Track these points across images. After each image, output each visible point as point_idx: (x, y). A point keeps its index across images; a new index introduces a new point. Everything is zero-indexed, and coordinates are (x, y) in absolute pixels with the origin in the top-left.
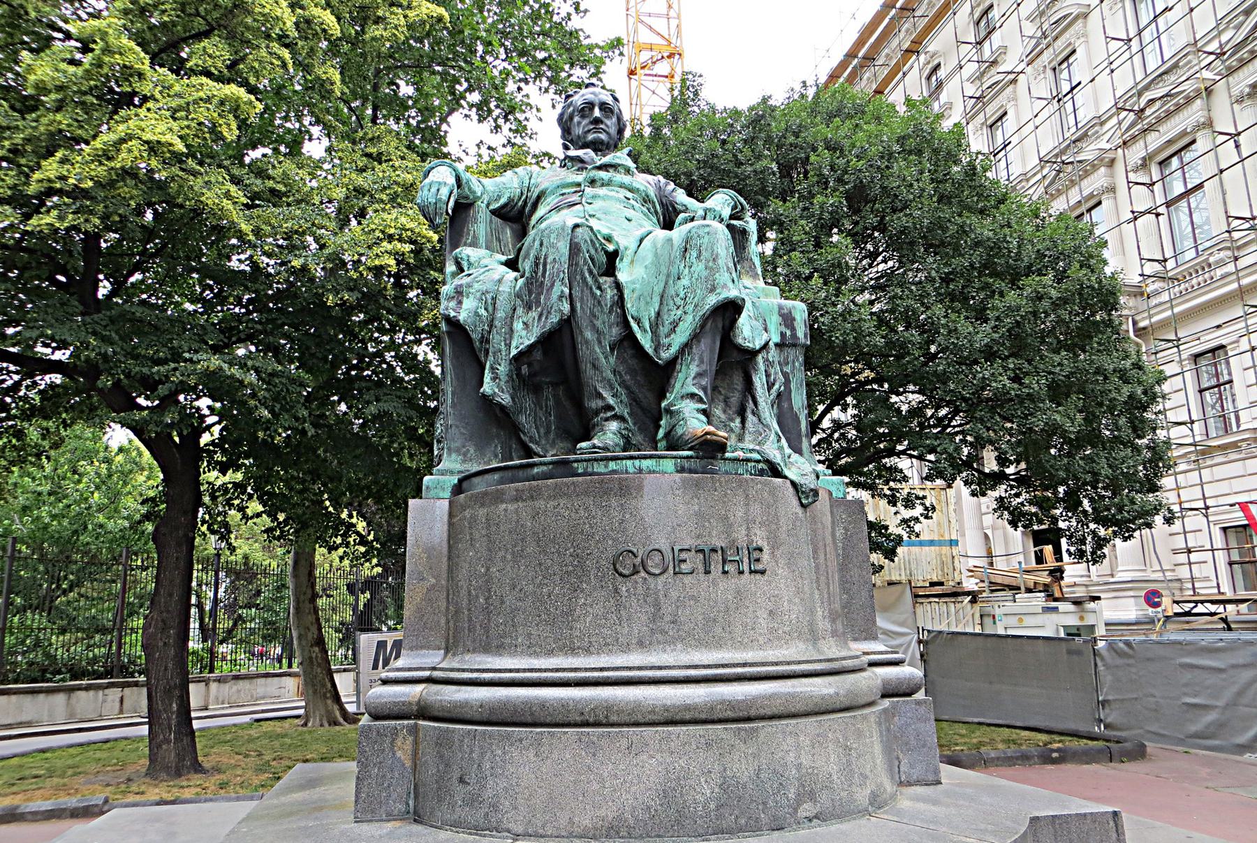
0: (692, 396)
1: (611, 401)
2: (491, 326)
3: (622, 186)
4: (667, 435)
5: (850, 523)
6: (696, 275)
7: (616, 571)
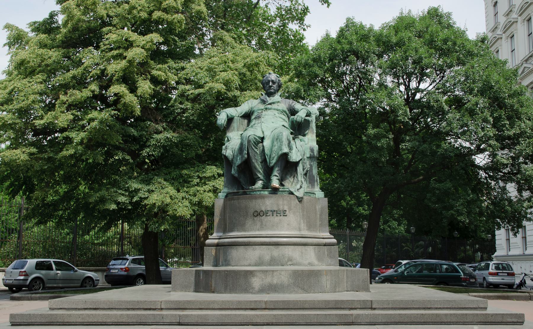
0: (276, 176)
3: (274, 109)
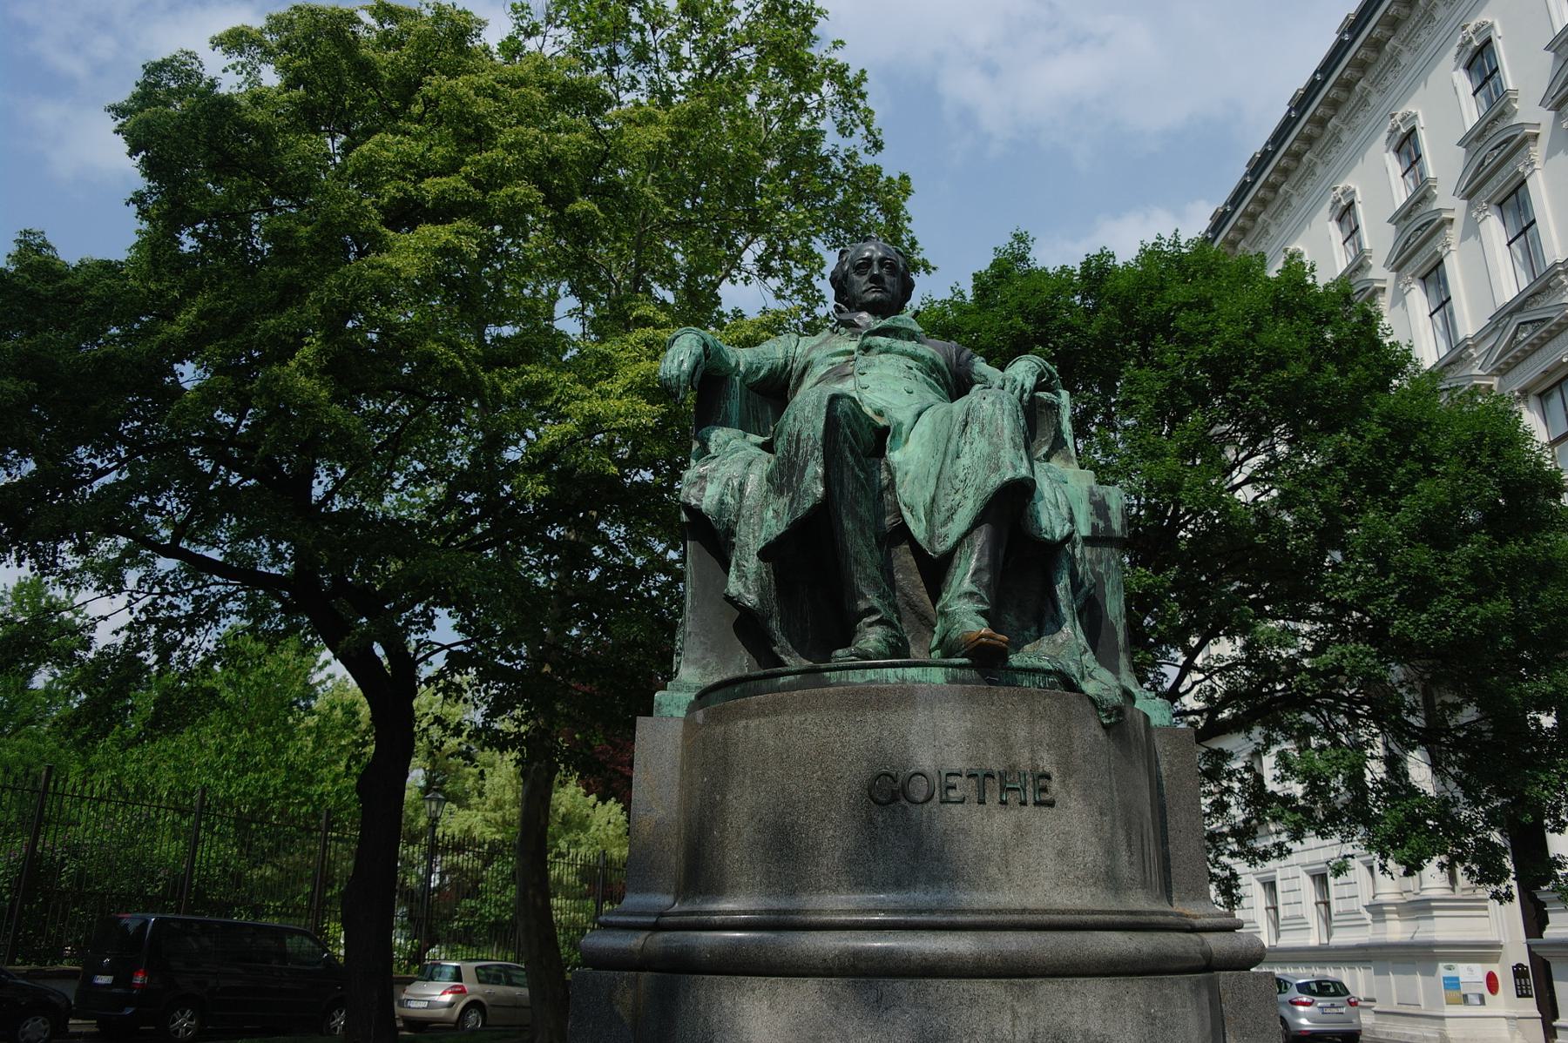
0: (971, 595)
1: (876, 603)
2: (738, 516)
3: (903, 353)
4: (941, 642)
5: (1176, 756)
6: (977, 453)
7: (871, 797)
